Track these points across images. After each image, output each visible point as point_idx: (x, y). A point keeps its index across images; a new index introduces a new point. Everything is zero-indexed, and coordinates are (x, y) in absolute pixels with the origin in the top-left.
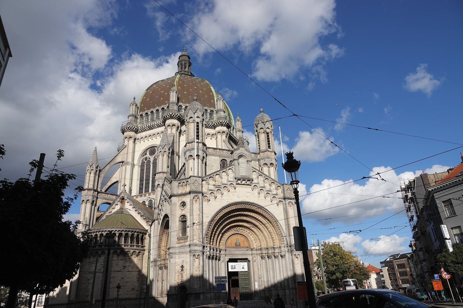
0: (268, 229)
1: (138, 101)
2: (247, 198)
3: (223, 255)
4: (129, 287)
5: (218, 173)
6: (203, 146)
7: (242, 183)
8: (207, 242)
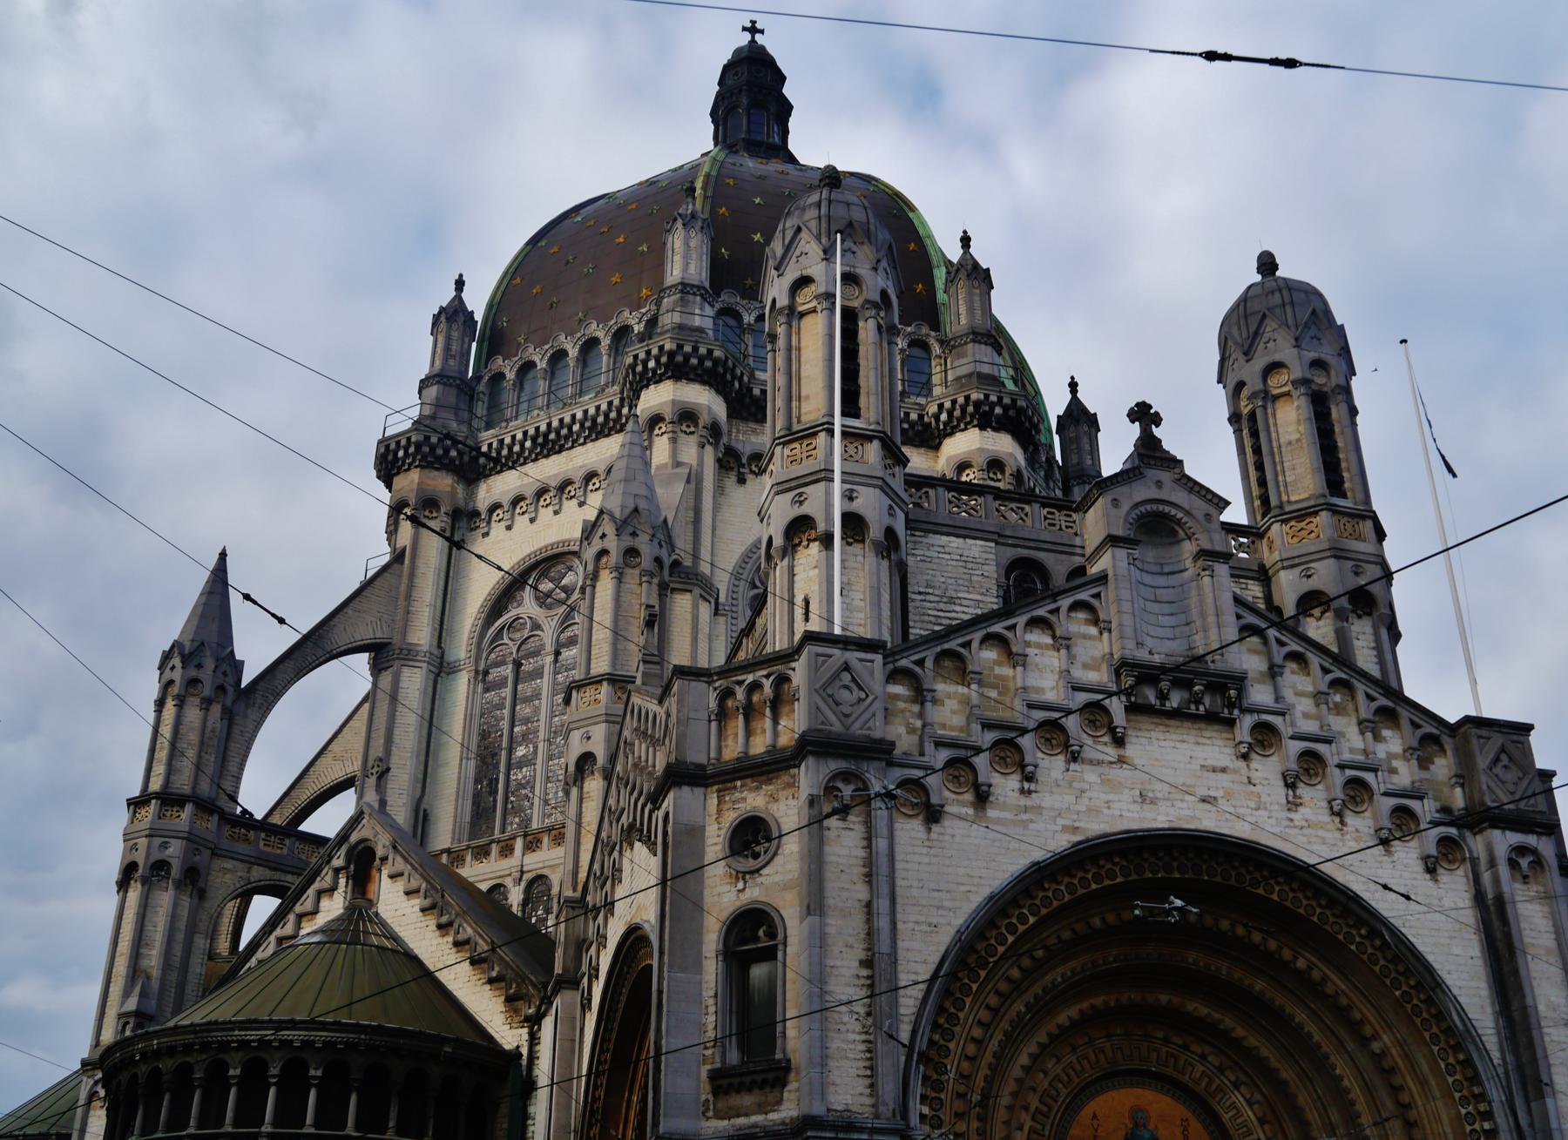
0: (1364, 1041)
1: (477, 302)
2: (1207, 806)
5: (997, 628)
6: (889, 461)
8: (926, 1110)
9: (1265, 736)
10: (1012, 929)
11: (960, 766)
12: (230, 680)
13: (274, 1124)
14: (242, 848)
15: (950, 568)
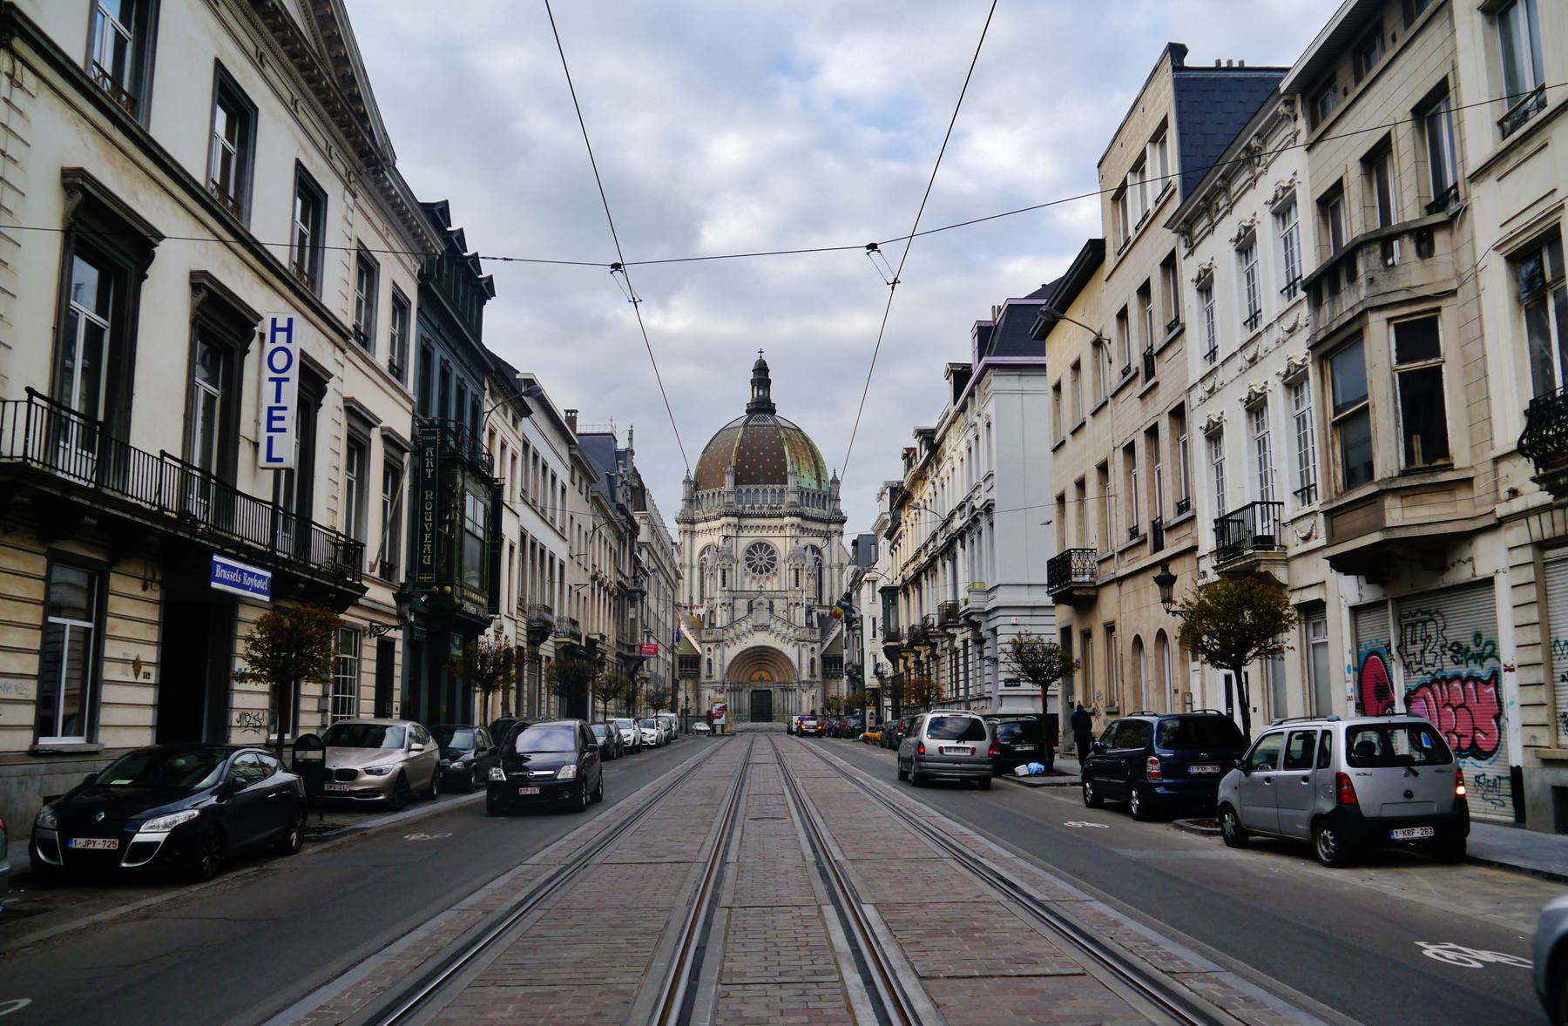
9: (772, 631)
11: (732, 640)
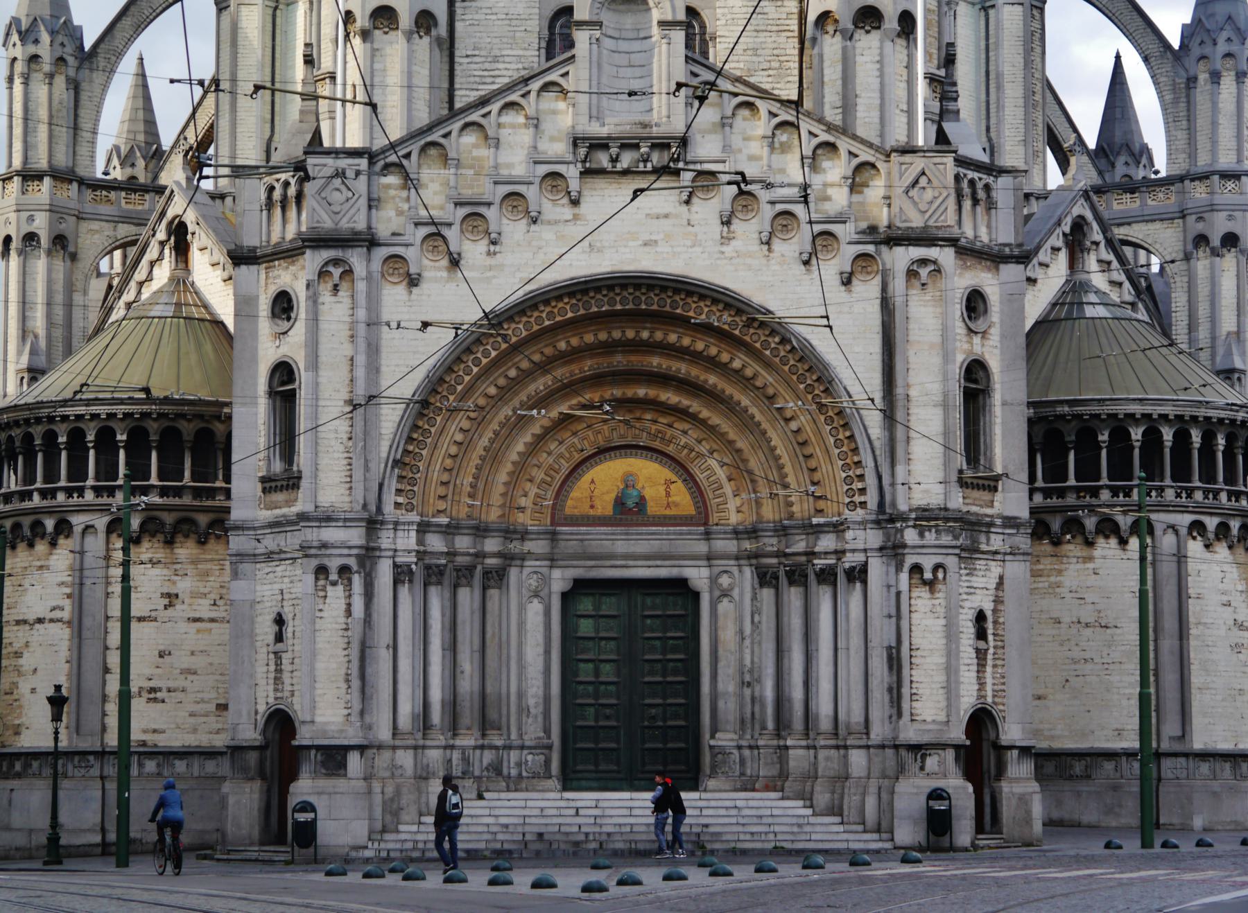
2: (647, 249)
3: (538, 563)
4: (200, 695)
5: (475, 117)
7: (619, 167)
8: (400, 500)
9: (706, 179)
10: (477, 362)
12: (69, 49)
13: (97, 478)
14: (104, 209)
15: (496, 29)
